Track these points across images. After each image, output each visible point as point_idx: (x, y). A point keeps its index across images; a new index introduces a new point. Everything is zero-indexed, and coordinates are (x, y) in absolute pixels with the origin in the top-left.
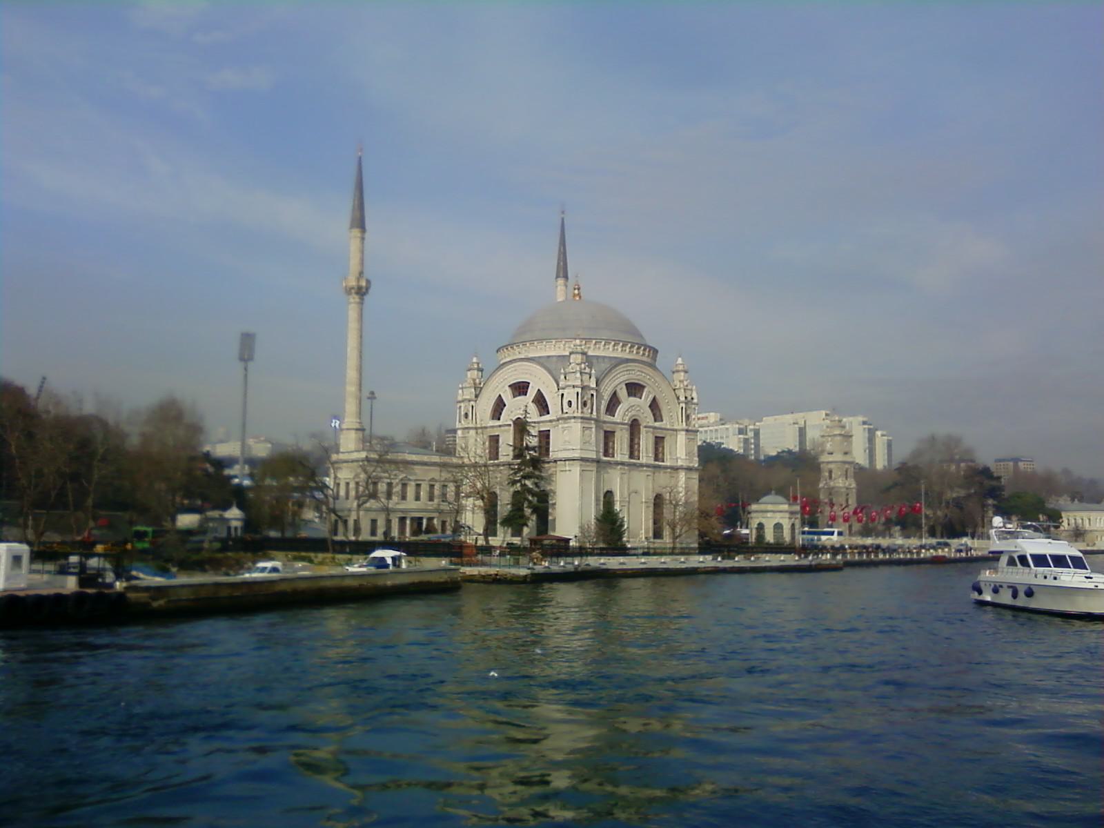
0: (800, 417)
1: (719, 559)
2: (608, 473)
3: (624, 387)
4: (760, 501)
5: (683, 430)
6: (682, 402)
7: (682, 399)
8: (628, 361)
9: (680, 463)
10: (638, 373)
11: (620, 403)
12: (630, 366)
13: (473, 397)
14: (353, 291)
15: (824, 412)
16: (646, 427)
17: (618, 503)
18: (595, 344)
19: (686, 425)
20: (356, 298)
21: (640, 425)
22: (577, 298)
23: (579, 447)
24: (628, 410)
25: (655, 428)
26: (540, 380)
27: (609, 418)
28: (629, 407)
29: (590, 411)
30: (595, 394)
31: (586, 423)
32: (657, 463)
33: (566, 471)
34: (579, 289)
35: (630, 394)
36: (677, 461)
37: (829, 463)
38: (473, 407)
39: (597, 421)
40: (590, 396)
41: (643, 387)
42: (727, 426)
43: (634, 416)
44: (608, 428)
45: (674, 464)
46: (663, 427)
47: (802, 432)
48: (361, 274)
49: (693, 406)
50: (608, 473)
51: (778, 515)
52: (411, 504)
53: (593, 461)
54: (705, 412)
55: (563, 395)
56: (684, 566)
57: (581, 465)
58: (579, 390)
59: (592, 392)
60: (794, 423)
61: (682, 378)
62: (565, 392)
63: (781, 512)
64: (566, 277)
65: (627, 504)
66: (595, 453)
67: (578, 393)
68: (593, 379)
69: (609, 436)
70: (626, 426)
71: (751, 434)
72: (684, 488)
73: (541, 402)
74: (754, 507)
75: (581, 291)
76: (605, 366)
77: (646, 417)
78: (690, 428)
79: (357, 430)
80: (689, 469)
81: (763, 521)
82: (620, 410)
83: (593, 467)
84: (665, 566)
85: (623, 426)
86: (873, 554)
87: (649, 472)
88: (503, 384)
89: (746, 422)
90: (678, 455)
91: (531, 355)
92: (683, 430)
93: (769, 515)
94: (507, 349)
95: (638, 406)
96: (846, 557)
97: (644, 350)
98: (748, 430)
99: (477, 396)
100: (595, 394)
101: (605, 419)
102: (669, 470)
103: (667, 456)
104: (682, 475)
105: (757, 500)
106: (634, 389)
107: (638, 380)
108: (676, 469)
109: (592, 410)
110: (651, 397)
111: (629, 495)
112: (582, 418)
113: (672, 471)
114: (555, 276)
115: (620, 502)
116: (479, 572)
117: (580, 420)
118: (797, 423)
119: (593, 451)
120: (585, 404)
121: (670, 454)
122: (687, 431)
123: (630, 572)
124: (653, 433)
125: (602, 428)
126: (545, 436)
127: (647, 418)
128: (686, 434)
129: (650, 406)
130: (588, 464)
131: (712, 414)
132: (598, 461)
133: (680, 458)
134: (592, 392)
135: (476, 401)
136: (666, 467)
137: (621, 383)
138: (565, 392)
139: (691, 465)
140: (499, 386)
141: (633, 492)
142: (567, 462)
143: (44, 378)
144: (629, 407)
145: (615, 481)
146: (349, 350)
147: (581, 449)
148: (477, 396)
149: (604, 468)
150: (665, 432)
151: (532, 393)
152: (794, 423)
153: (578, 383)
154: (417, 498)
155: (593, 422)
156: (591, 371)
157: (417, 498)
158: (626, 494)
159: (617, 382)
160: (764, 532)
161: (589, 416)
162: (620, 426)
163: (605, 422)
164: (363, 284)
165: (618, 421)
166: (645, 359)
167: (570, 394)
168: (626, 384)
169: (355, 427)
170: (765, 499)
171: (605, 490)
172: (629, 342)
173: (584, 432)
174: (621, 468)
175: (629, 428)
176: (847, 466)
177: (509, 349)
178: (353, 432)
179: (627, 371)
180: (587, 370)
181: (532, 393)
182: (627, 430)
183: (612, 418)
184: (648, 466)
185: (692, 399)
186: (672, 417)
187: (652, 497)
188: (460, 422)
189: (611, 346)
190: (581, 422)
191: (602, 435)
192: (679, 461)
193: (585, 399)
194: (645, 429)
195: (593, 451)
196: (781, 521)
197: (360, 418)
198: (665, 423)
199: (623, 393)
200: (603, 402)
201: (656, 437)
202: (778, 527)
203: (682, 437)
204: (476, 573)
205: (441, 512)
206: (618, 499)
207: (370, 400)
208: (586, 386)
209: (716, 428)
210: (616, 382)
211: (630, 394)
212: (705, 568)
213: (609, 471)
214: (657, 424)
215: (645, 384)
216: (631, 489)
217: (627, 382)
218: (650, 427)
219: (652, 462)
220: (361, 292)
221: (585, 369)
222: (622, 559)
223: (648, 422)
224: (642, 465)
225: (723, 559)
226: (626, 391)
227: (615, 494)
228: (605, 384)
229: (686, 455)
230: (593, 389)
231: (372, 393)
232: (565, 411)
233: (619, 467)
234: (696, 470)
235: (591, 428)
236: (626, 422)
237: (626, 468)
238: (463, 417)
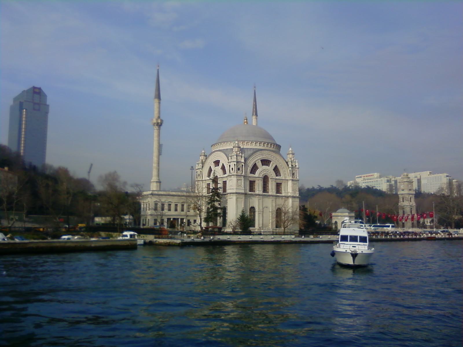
0: (418, 174)
1: (303, 237)
2: (252, 199)
3: (260, 161)
4: (337, 211)
5: (290, 180)
6: (290, 168)
7: (290, 166)
8: (261, 150)
9: (289, 194)
10: (267, 155)
11: (258, 169)
12: (264, 152)
13: (201, 167)
14: (155, 125)
15: (428, 172)
16: (271, 179)
17: (257, 212)
18: (247, 143)
19: (292, 178)
20: (157, 128)
21: (269, 178)
22: (246, 124)
23: (235, 188)
24: (262, 171)
25: (276, 179)
26: (224, 160)
27: (252, 175)
28: (262, 170)
29: (241, 172)
30: (243, 165)
31: (239, 177)
32: (277, 194)
33: (230, 198)
34: (247, 120)
35: (263, 165)
36: (288, 194)
37: (402, 194)
38: (201, 171)
39: (244, 176)
40: (241, 166)
41: (271, 161)
42: (381, 179)
43: (265, 174)
44: (252, 179)
45: (286, 195)
46: (280, 178)
47: (419, 181)
48: (159, 117)
49: (296, 169)
50: (252, 199)
52: (173, 212)
53: (242, 194)
54: (373, 173)
55: (230, 165)
56: (273, 240)
57: (236, 196)
58: (236, 163)
59: (242, 164)
60: (415, 177)
61: (291, 157)
62: (231, 164)
64: (256, 115)
65: (262, 212)
66: (244, 190)
67: (235, 165)
68: (243, 158)
69: (252, 184)
70: (261, 179)
71: (393, 183)
72: (291, 206)
73: (223, 168)
74: (333, 214)
75: (248, 120)
76: (250, 152)
77: (272, 174)
78: (294, 179)
79: (157, 182)
80: (293, 197)
81: (337, 220)
82: (258, 172)
83: (243, 196)
84: (262, 240)
85: (259, 179)
86: (393, 236)
87: (274, 198)
88: (211, 161)
89: (391, 177)
90: (289, 191)
91: (221, 149)
92: (290, 180)
93: (339, 218)
94: (216, 145)
95: (267, 170)
96: (378, 237)
97: (274, 145)
98: (391, 180)
99: (202, 167)
100: (243, 165)
101: (249, 176)
102: (284, 198)
103: (283, 191)
104: (290, 200)
105: (335, 211)
106: (266, 162)
107: (267, 158)
108: (288, 197)
109: (242, 172)
110: (274, 166)
111: (263, 209)
112: (236, 175)
113: (286, 198)
114: (252, 115)
115: (258, 211)
116: (164, 241)
117: (236, 176)
118: (416, 177)
119: (243, 189)
121: (285, 190)
122: (292, 180)
123: (243, 242)
124: (275, 181)
125: (249, 179)
126: (225, 183)
127: (272, 174)
128: (292, 182)
129: (274, 170)
130: (240, 195)
131: (376, 173)
132: (245, 194)
133: (289, 192)
134: (242, 164)
135: (202, 169)
136: (282, 197)
137: (259, 159)
138: (231, 164)
139: (295, 195)
140: (210, 163)
141: (265, 207)
142: (231, 194)
143: (92, 165)
144: (262, 170)
145: (255, 202)
146: (154, 148)
147: (236, 189)
148: (202, 167)
149: (250, 197)
150: (281, 181)
151: (221, 165)
152: (415, 177)
153: (235, 160)
154: (176, 210)
155: (242, 177)
156: (242, 154)
157: (176, 210)
158: (261, 208)
159: (256, 159)
160: (337, 225)
161: (240, 174)
162: (257, 178)
163: (250, 177)
164: (159, 121)
165: (257, 176)
166: (271, 149)
167: (232, 166)
168: (261, 160)
169: (155, 181)
170: (339, 211)
171: (251, 206)
172: (262, 142)
173: (238, 181)
174: (258, 197)
175: (263, 179)
176: (411, 196)
177: (215, 146)
178: (155, 183)
179: (261, 154)
180: (241, 154)
181: (221, 165)
182: (261, 180)
183: (254, 175)
184: (272, 196)
185: (296, 166)
186: (285, 173)
187: (275, 209)
188: (197, 178)
189: (254, 144)
190: (236, 177)
191: (248, 183)
192: (289, 193)
193: (239, 167)
194: (271, 180)
195: (243, 189)
197: (159, 177)
198: (282, 177)
199: (259, 164)
200: (249, 168)
203: (290, 183)
204: (163, 242)
205: (187, 216)
206: (257, 210)
207: (191, 170)
208: (239, 161)
209: (377, 180)
210: (256, 159)
211: (263, 165)
212: (284, 241)
213: (252, 198)
214: (277, 177)
215: (271, 160)
216: (264, 206)
217: (261, 159)
218: (274, 179)
219: (275, 194)
220: (159, 125)
221: (239, 154)
222: (251, 237)
223: (273, 177)
224: (269, 196)
225: (305, 237)
226: (261, 163)
227: (255, 208)
228: (250, 160)
229: (292, 191)
230: (242, 162)
231: (192, 167)
232: (231, 172)
233: (257, 196)
234: (297, 197)
235: (242, 180)
236: (261, 176)
237: (261, 197)
238: (198, 176)
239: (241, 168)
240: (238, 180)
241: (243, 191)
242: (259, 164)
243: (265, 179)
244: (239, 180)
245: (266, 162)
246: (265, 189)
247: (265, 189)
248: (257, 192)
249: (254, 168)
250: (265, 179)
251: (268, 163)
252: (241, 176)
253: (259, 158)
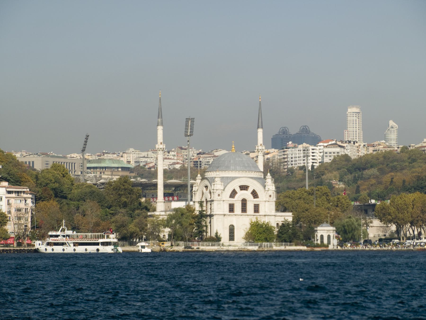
3: (239, 188)
28: (241, 195)
35: (241, 190)
51: (322, 231)
63: (322, 230)
82: (237, 196)
106: (244, 188)
120: (219, 195)
132: (225, 215)
175: (241, 202)
196: (323, 234)
199: (238, 190)
201: (254, 204)
202: (322, 237)
210: (235, 185)
211: (241, 190)
239: (221, 195)
240: (218, 204)
241: (222, 213)
242: (238, 190)
243: (244, 203)
244: (218, 204)
245: (244, 188)
246: (244, 209)
247: (244, 209)
248: (235, 213)
249: (233, 194)
250: (244, 203)
251: (247, 188)
252: (221, 200)
253: (237, 185)
